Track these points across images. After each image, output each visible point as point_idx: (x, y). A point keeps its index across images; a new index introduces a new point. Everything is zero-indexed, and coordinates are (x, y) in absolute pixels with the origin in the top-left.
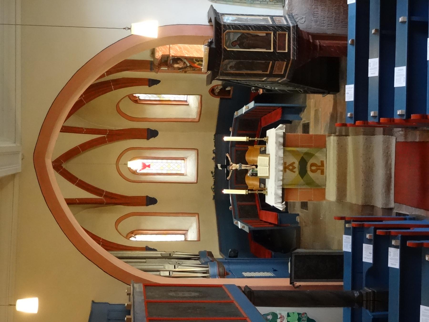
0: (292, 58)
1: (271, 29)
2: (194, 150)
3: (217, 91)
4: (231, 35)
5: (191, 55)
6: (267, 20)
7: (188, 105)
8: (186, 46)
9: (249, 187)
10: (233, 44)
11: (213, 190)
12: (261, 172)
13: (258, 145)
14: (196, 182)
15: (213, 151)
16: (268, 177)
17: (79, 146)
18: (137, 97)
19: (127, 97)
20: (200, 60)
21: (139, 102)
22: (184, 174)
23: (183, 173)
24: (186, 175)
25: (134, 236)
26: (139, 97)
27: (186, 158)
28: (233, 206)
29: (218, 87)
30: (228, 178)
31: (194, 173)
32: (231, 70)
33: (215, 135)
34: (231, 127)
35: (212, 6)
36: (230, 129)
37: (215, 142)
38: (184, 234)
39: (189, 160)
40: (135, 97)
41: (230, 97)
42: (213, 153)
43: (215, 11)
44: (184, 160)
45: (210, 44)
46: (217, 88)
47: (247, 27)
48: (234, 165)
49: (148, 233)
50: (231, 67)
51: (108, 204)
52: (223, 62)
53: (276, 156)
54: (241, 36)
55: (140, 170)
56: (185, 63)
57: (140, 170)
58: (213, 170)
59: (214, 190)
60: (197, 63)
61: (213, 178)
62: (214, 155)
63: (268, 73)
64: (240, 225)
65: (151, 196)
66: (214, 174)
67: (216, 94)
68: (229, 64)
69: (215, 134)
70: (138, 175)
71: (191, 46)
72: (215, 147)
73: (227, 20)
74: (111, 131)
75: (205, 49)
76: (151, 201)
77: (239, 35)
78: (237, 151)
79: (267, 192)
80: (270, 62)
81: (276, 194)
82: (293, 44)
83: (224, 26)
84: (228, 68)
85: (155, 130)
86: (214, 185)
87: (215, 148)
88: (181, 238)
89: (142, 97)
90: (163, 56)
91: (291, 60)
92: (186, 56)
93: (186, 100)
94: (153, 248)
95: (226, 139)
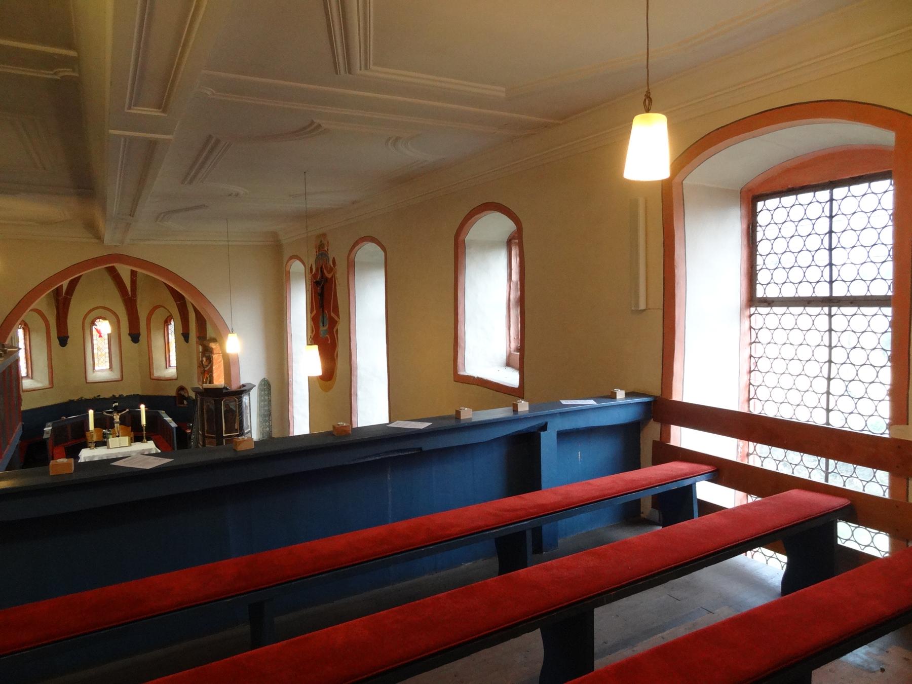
3: (182, 393)
4: (234, 403)
5: (214, 371)
6: (247, 429)
7: (166, 368)
8: (222, 367)
10: (227, 406)
12: (112, 441)
13: (134, 436)
16: (109, 448)
17: (118, 273)
19: (169, 314)
20: (211, 382)
24: (94, 372)
25: (23, 326)
30: (105, 413)
33: (138, 395)
34: (149, 409)
35: (255, 386)
37: (131, 395)
38: (27, 376)
40: (170, 321)
43: (251, 389)
44: (110, 368)
45: (225, 388)
47: (241, 414)
48: (118, 417)
50: (209, 405)
51: (57, 301)
53: (131, 452)
56: (207, 366)
60: (208, 376)
62: (117, 396)
63: (206, 435)
64: (48, 429)
65: (69, 340)
66: (98, 398)
67: (179, 392)
71: (223, 370)
73: (245, 399)
74: (135, 301)
75: (221, 385)
76: (63, 341)
77: (235, 409)
79: (93, 449)
81: (94, 456)
83: (241, 397)
87: (125, 396)
88: (23, 372)
89: (171, 327)
90: (212, 349)
92: (214, 368)
95: (143, 407)
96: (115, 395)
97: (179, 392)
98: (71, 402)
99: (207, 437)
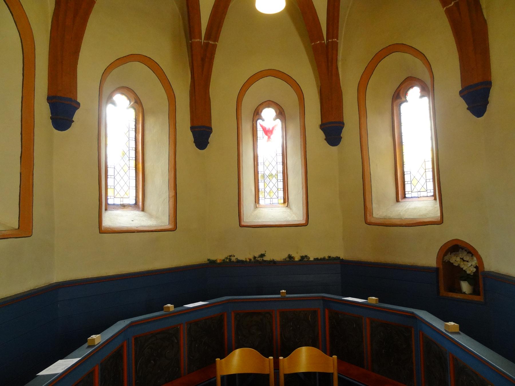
2: (305, 217)
3: (455, 260)
7: (398, 201)
9: (223, 360)
11: (227, 258)
14: (243, 224)
15: (306, 256)
18: (405, 98)
21: (395, 105)
22: (258, 203)
23: (262, 202)
24: (256, 207)
26: (406, 101)
27: (287, 206)
28: (173, 312)
29: (464, 261)
31: (260, 221)
33: (338, 258)
34: (380, 301)
36: (374, 298)
37: (324, 259)
38: (136, 204)
39: (285, 212)
40: (406, 94)
41: (443, 293)
42: (301, 255)
44: (284, 202)
46: (462, 259)
49: (139, 132)
51: (191, 47)
55: (261, 126)
57: (261, 126)
58: (267, 258)
59: (228, 260)
61: (251, 257)
65: (212, 138)
67: (446, 258)
69: (341, 258)
70: (253, 121)
72: (314, 259)
78: (315, 312)
85: (341, 138)
86: (239, 262)
87: (312, 259)
93: (407, 196)
94: (75, 118)
96: (293, 255)
97: (446, 258)
98: (212, 263)
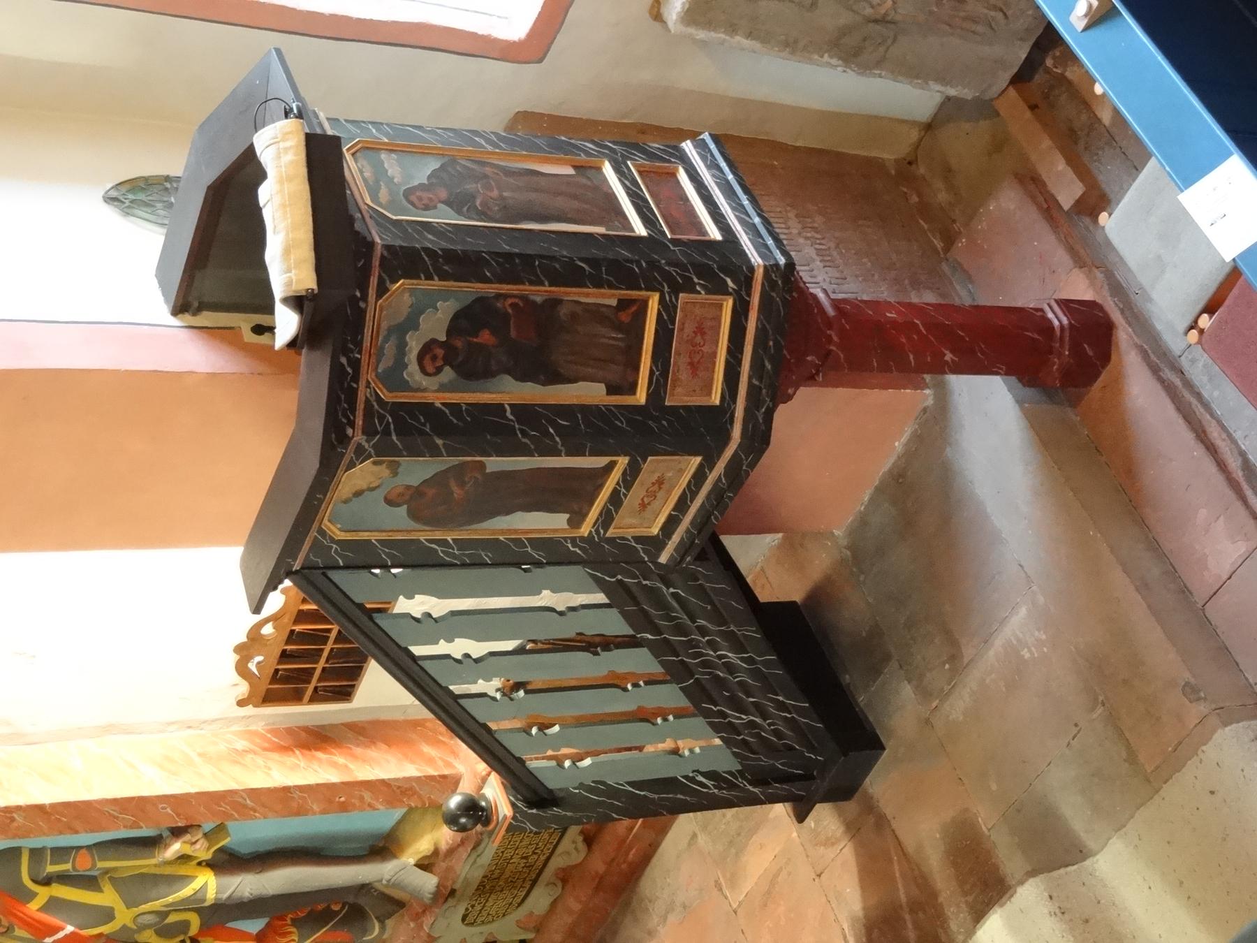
0: (760, 261)
1: (590, 148)
32: (425, 381)
50: (427, 349)
52: (379, 296)
54: (442, 167)
63: (641, 397)
68: (411, 323)
80: (644, 304)
82: (733, 209)
84: (412, 371)
91: (759, 275)
99: (657, 391)
